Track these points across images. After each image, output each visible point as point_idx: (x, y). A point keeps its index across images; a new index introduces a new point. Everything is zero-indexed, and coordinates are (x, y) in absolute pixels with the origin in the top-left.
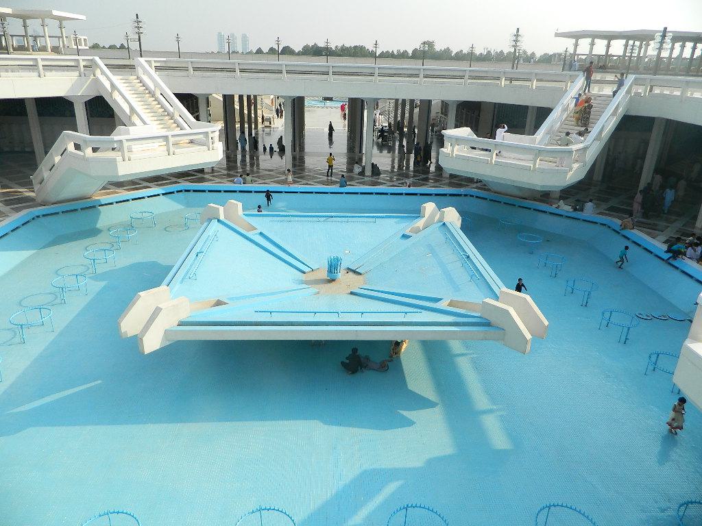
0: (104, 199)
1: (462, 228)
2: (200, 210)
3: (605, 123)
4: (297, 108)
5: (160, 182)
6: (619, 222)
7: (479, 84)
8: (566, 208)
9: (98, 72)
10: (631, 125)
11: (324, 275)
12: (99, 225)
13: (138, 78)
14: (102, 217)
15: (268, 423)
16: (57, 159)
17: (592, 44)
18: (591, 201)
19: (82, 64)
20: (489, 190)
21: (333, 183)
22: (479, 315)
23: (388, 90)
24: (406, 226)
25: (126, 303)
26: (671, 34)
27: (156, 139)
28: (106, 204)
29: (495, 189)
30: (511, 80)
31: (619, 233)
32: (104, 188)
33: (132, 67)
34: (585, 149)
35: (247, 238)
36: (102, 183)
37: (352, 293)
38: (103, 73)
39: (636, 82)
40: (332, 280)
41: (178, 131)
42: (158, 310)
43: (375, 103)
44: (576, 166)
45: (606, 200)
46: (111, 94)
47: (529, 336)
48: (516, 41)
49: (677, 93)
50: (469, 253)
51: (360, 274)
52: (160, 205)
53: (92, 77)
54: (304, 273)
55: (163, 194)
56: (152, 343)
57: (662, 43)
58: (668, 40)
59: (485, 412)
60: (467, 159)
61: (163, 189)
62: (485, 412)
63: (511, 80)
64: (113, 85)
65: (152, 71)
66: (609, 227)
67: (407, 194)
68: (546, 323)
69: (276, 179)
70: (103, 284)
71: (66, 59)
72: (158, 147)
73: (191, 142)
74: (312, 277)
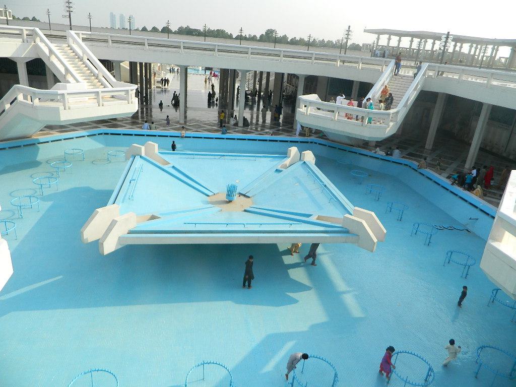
0: (42, 138)
1: (316, 164)
2: (124, 149)
3: (410, 95)
4: (184, 73)
5: (83, 127)
6: (417, 164)
7: (321, 63)
8: (380, 153)
9: (38, 40)
10: (426, 98)
11: (224, 198)
12: (39, 158)
13: (69, 46)
14: (40, 151)
15: (194, 304)
16: (7, 106)
17: (389, 39)
18: (397, 148)
19: (25, 33)
20: (327, 139)
21: (216, 131)
22: (341, 225)
23: (249, 63)
24: (278, 163)
25: (87, 215)
26: (451, 37)
27: (87, 93)
28: (42, 143)
29: (331, 137)
30: (344, 62)
31: (417, 171)
32: (41, 131)
33: (64, 37)
34: (397, 113)
35: (163, 170)
36: (42, 126)
37: (245, 211)
38: (42, 40)
39: (429, 68)
40: (230, 202)
41: (101, 89)
42: (114, 223)
43: (245, 72)
44: (391, 124)
45: (406, 149)
46: (49, 57)
47: (375, 240)
48: (348, 35)
49: (456, 77)
50: (325, 183)
51: (249, 197)
52: (87, 144)
53: (33, 43)
54: (208, 196)
55: (88, 136)
56: (109, 247)
57: (446, 42)
58: (449, 40)
59: (344, 293)
60: (315, 116)
61: (88, 132)
62: (344, 293)
63: (344, 62)
64: (51, 51)
65: (80, 41)
66: (410, 167)
67: (270, 141)
68: (385, 231)
69: (174, 127)
70: (50, 204)
71: (14, 28)
72: (89, 101)
73: (113, 97)
74: (214, 199)
